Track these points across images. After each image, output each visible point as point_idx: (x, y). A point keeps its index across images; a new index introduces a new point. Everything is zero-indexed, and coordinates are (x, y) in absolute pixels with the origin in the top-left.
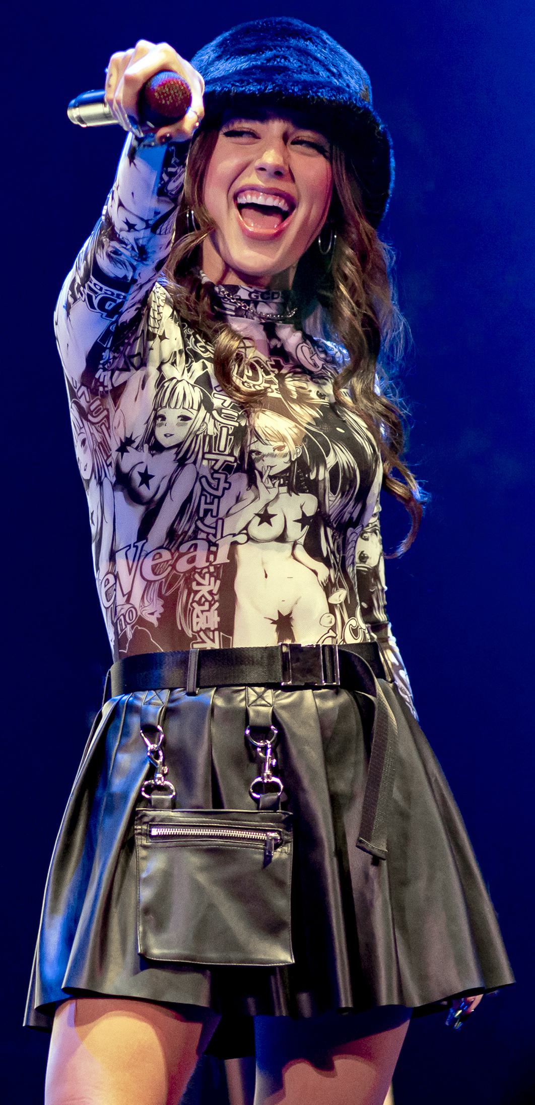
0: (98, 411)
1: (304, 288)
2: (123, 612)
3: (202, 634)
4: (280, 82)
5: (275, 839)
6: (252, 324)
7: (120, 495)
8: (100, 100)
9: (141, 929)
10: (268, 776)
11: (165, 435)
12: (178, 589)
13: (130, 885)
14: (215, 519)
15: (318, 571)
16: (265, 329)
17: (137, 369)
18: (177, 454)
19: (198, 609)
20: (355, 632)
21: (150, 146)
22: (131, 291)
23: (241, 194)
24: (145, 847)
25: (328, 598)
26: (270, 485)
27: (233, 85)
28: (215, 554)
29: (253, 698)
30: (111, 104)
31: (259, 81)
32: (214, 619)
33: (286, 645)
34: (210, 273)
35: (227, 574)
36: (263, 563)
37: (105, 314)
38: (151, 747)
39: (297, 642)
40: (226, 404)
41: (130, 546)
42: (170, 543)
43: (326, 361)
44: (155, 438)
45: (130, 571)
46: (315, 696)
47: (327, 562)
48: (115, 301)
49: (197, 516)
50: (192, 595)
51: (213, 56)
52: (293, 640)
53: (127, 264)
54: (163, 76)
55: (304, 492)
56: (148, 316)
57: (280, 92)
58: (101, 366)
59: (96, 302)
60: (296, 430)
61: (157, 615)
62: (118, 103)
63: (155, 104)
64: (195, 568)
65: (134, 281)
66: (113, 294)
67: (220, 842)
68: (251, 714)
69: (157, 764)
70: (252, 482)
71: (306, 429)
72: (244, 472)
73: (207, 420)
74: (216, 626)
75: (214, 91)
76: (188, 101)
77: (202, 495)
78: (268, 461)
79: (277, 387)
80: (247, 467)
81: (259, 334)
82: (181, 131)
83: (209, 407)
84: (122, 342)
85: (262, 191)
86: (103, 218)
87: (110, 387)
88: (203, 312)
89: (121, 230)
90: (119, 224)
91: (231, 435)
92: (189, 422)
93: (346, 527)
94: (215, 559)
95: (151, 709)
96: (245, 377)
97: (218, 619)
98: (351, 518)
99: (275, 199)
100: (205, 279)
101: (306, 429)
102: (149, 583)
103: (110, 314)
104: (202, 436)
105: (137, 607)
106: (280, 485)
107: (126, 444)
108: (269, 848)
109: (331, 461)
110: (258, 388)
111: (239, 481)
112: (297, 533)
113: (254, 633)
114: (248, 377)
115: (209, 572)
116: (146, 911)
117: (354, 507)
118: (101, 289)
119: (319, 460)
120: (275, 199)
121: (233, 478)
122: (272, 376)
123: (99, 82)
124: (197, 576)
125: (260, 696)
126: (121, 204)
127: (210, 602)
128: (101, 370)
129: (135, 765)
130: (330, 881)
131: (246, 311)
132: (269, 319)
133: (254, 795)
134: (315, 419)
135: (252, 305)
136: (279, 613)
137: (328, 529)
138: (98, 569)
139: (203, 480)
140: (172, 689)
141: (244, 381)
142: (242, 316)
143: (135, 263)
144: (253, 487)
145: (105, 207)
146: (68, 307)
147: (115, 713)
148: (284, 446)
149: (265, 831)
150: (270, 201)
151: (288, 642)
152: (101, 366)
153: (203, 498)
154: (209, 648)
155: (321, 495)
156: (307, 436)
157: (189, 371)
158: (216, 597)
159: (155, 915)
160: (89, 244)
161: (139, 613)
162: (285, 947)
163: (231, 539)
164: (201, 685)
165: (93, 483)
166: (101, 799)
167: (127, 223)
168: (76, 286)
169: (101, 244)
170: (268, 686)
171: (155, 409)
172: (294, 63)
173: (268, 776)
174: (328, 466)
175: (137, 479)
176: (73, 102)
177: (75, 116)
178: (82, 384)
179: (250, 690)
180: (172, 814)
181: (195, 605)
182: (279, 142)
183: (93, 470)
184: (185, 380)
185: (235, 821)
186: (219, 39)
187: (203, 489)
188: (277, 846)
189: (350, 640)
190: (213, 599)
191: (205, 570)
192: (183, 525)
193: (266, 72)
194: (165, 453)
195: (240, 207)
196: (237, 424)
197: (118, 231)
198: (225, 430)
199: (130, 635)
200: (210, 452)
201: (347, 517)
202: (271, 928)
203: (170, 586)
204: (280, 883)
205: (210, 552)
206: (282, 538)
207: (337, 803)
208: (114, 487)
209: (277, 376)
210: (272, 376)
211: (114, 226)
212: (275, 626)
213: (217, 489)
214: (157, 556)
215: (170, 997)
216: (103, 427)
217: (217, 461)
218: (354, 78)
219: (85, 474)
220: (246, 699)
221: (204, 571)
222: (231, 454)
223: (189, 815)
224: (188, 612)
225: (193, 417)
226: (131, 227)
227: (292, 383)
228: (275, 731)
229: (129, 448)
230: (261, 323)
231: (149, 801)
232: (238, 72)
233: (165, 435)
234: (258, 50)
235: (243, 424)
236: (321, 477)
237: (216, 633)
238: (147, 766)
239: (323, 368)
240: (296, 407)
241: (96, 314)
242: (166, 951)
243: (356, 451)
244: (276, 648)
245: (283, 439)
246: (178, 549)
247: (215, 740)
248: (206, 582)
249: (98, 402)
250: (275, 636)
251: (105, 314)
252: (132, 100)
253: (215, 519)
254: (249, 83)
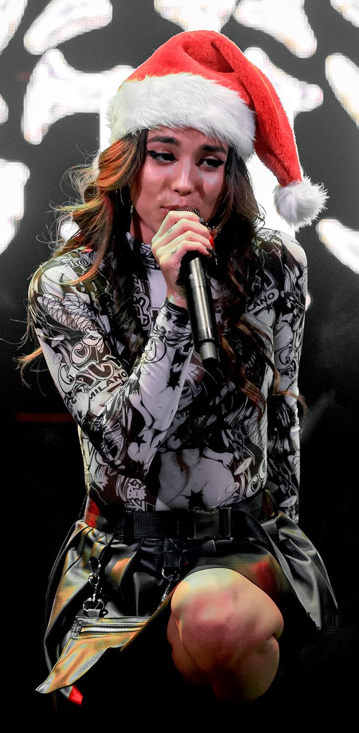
3: (133, 501)
19: (131, 487)
61: (103, 484)
74: (144, 499)
127: (140, 485)
181: (129, 484)
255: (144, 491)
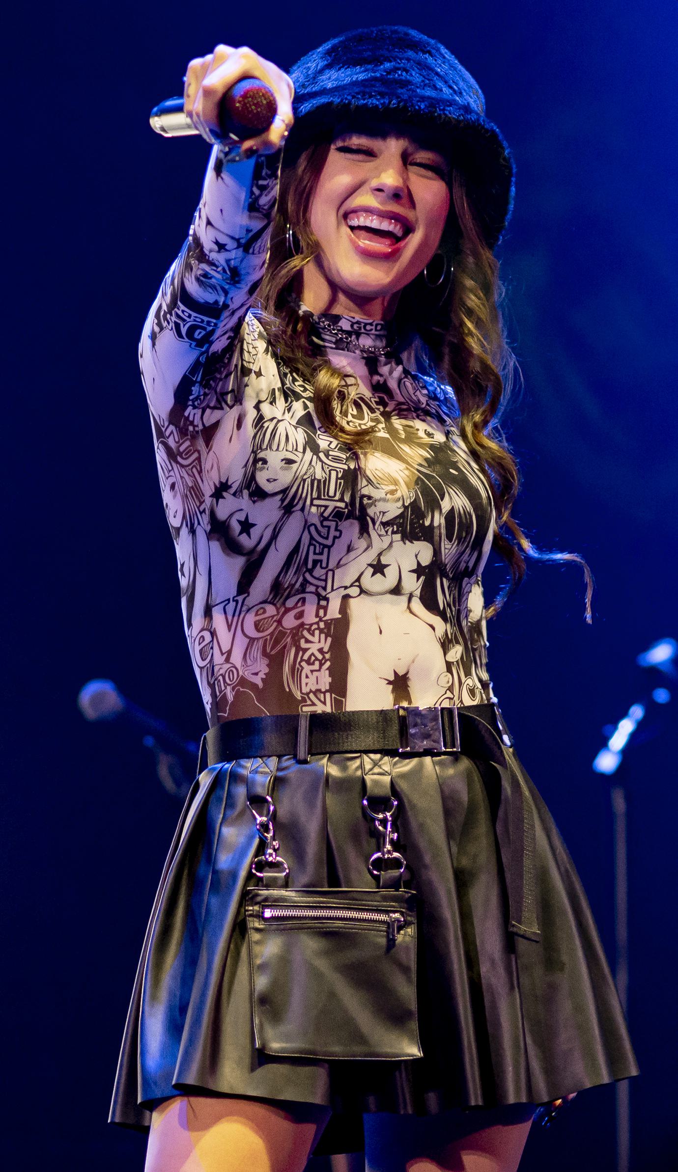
0: (188, 453)
1: (416, 321)
2: (222, 672)
3: (312, 696)
4: (405, 97)
5: (399, 921)
6: (355, 358)
7: (216, 546)
8: (179, 109)
9: (257, 1021)
10: (388, 851)
11: (268, 480)
12: (285, 647)
13: (243, 971)
14: (324, 571)
15: (434, 625)
16: (367, 364)
17: (231, 407)
18: (282, 500)
19: (307, 668)
20: (472, 692)
21: (234, 161)
22: (222, 318)
23: (351, 215)
24: (258, 930)
25: (445, 654)
26: (383, 532)
27: (354, 97)
28: (325, 608)
29: (368, 766)
30: (190, 114)
31: (382, 95)
32: (325, 680)
33: (403, 708)
34: (313, 300)
35: (338, 631)
36: (377, 618)
37: (194, 344)
38: (259, 819)
39: (414, 705)
40: (333, 446)
41: (229, 600)
42: (275, 597)
43: (430, 398)
44: (256, 483)
45: (229, 627)
46: (434, 763)
47: (443, 615)
48: (204, 329)
49: (305, 568)
50: (301, 653)
51: (322, 64)
52: (410, 702)
53: (218, 288)
54: (246, 85)
55: (418, 539)
56: (242, 350)
57: (405, 107)
58: (190, 403)
59: (184, 331)
60: (407, 472)
61: (262, 675)
62: (198, 115)
63: (239, 113)
64: (302, 625)
65: (226, 306)
66: (202, 321)
67: (339, 923)
68: (369, 783)
69: (266, 837)
70: (364, 530)
71: (418, 471)
72: (355, 518)
73: (314, 463)
75: (331, 103)
76: (272, 109)
77: (310, 544)
78: (381, 506)
79: (383, 425)
80: (358, 513)
81: (361, 369)
82: (268, 144)
83: (316, 449)
84: (212, 376)
85: (365, 211)
86: (190, 238)
87: (201, 427)
88: (300, 346)
89: (211, 251)
90: (208, 244)
91: (341, 479)
92: (295, 466)
93: (459, 578)
94: (325, 614)
95: (259, 778)
96: (349, 416)
97: (330, 680)
98: (467, 567)
99: (390, 223)
100: (304, 308)
101: (418, 471)
102: (252, 640)
103: (200, 343)
104: (309, 480)
105: (239, 667)
106: (393, 533)
107: (221, 489)
108: (391, 929)
109: (446, 505)
110: (364, 427)
111: (351, 529)
112: (413, 584)
113: (368, 694)
114: (353, 416)
115: (319, 628)
116: (264, 1000)
117: (471, 555)
118: (190, 316)
119: (434, 505)
120: (390, 223)
121: (344, 525)
122: (378, 413)
123: (179, 90)
124: (305, 633)
125: (375, 764)
126: (209, 223)
127: (320, 661)
128: (190, 408)
129: (242, 839)
130: (456, 966)
131: (348, 343)
132: (371, 352)
133: (375, 872)
134: (426, 460)
135: (354, 337)
136: (395, 673)
137: (445, 580)
138: (190, 625)
139: (312, 529)
140: (280, 757)
141: (351, 421)
142: (343, 349)
143: (227, 287)
144: (365, 535)
145: (192, 227)
146: (153, 337)
147: (216, 784)
148: (396, 490)
149: (387, 912)
150: (386, 226)
151: (405, 704)
152: (190, 403)
153: (312, 548)
154: (320, 712)
155: (436, 543)
156: (419, 478)
157: (289, 410)
158: (327, 656)
159: (269, 1004)
160: (175, 267)
161: (241, 673)
162: (411, 1039)
163: (343, 592)
164: (314, 751)
165: (184, 531)
166: (206, 877)
167: (217, 243)
168: (162, 313)
169: (188, 267)
170: (385, 752)
171: (253, 452)
172: (416, 77)
173: (388, 851)
174: (444, 511)
175: (236, 527)
176: (155, 109)
177: (158, 126)
178: (170, 423)
179: (365, 756)
180: (287, 893)
181: (304, 664)
182: (397, 161)
183: (184, 517)
184: (287, 421)
185: (354, 901)
186: (327, 46)
187: (312, 538)
188: (400, 928)
189: (468, 702)
190: (324, 657)
191: (315, 626)
192: (290, 578)
193: (389, 85)
194: (268, 501)
195: (352, 228)
196: (346, 467)
197: (207, 252)
198: (334, 474)
199: (230, 697)
200: (319, 498)
201: (463, 566)
202: (395, 1017)
203: (277, 642)
204: (405, 970)
205: (319, 607)
206: (396, 591)
207: (463, 880)
208: (209, 536)
209: (382, 414)
210: (378, 413)
211: (202, 247)
212: (391, 687)
213: (327, 538)
214: (262, 611)
215: (289, 1095)
216: (194, 470)
217: (326, 507)
218: (465, 92)
219: (174, 521)
220: (361, 766)
221: (313, 628)
222: (341, 500)
223: (305, 894)
224: (295, 671)
225: (298, 459)
226: (221, 247)
227: (398, 421)
228: (392, 800)
229: (224, 494)
230: (364, 358)
231: (261, 879)
232: (354, 84)
233: (268, 480)
234: (377, 61)
235: (352, 467)
236: (436, 524)
237: (328, 695)
238: (257, 841)
239: (428, 404)
240: (406, 448)
241: (185, 344)
242: (284, 1045)
243: (471, 493)
244: (393, 711)
245: (395, 482)
246: (284, 604)
247: (330, 812)
248: (315, 639)
249: (187, 443)
250: (390, 698)
251: (194, 344)
252: (212, 112)
253: (324, 571)
254: (371, 96)
255: (327, 672)
